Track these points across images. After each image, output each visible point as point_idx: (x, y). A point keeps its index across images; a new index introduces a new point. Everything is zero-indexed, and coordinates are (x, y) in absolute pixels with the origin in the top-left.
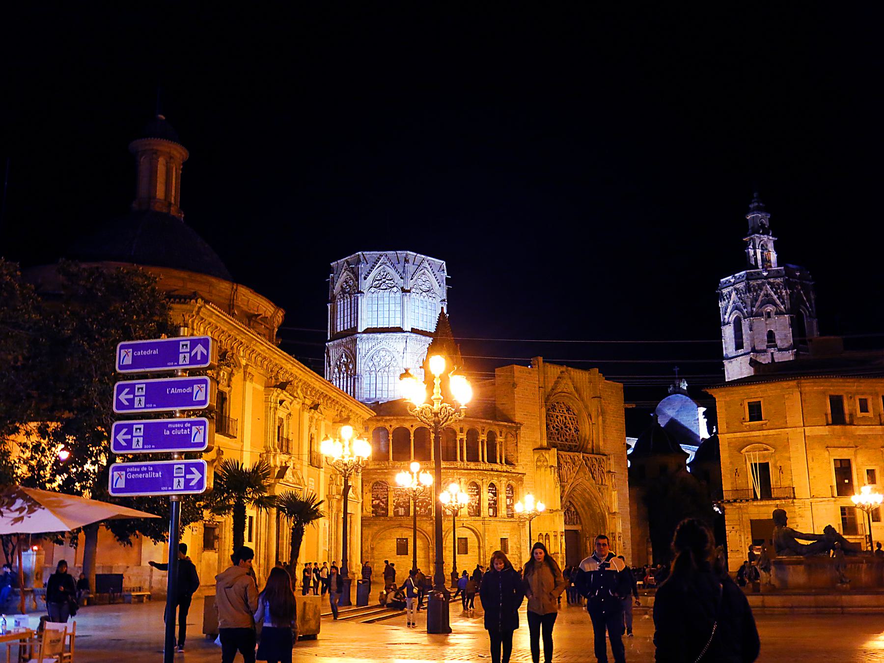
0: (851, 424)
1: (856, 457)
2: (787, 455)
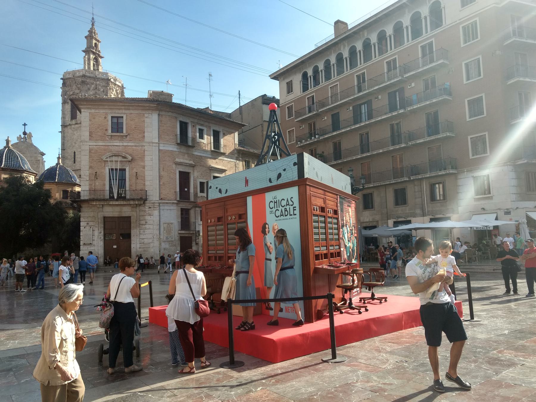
0: (193, 147)
1: (194, 171)
2: (142, 164)
